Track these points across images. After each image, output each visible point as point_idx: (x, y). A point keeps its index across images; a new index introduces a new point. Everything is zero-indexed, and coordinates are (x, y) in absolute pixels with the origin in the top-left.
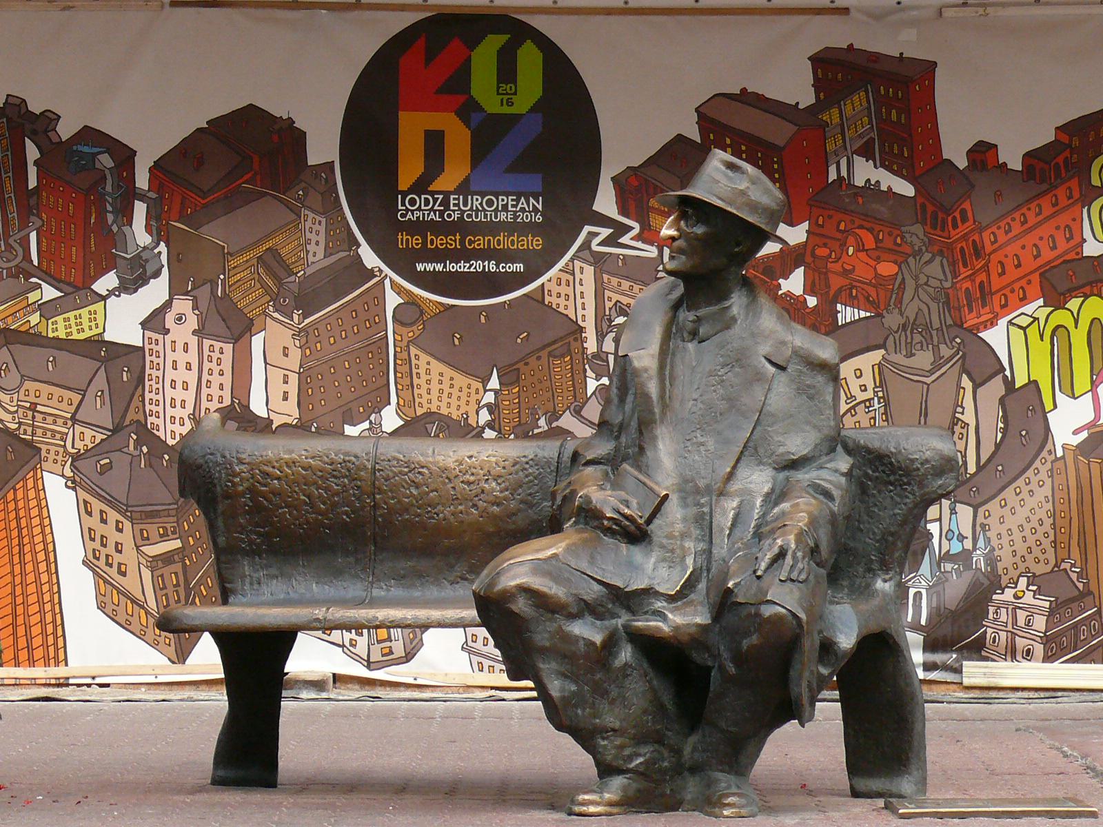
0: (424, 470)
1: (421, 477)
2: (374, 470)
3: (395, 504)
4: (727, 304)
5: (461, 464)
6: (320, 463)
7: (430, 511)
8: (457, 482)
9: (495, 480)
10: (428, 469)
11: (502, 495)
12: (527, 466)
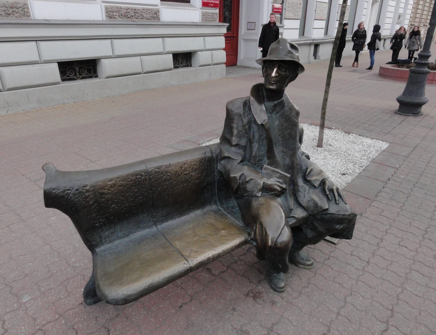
0: (168, 174)
2: (150, 179)
4: (283, 99)
5: (182, 168)
7: (174, 189)
10: (171, 173)
11: (199, 176)
12: (205, 162)
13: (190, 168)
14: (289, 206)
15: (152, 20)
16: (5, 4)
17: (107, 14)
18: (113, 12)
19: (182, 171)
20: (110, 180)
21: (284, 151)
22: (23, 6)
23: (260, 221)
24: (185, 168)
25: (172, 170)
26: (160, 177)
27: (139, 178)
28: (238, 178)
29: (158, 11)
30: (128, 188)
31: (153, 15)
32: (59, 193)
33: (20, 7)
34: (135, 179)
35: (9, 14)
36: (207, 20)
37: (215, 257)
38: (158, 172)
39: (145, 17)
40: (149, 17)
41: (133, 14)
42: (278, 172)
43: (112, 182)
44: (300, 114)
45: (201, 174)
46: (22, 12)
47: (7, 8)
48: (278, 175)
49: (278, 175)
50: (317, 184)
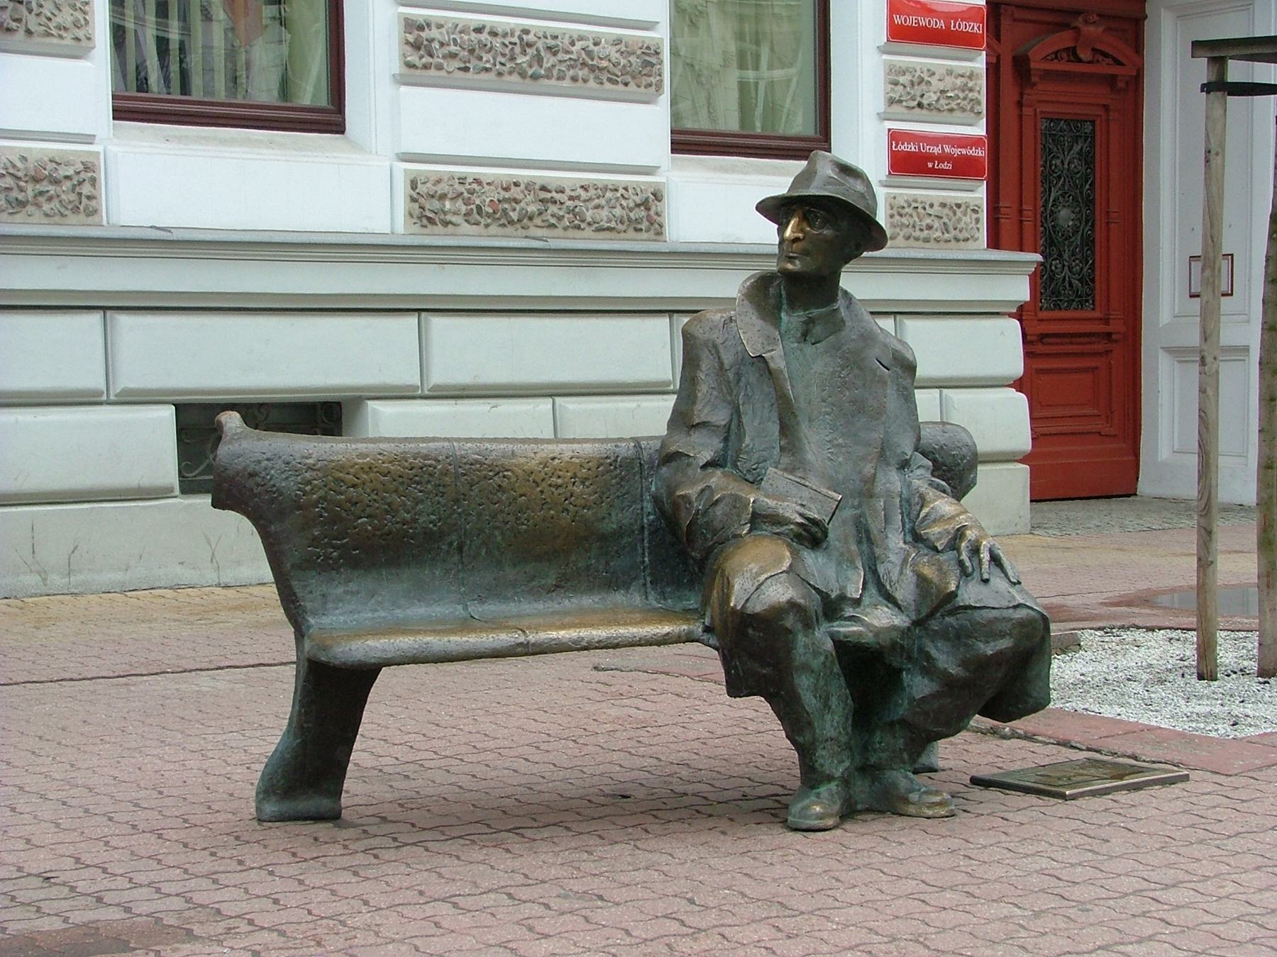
5: (546, 466)
9: (583, 483)
10: (512, 472)
15: (622, 235)
16: (14, 166)
17: (416, 205)
18: (443, 197)
22: (78, 173)
27: (430, 466)
29: (658, 196)
31: (631, 210)
33: (67, 177)
35: (22, 204)
36: (917, 239)
38: (482, 464)
39: (589, 219)
40: (609, 221)
41: (532, 208)
46: (73, 197)
47: (19, 178)
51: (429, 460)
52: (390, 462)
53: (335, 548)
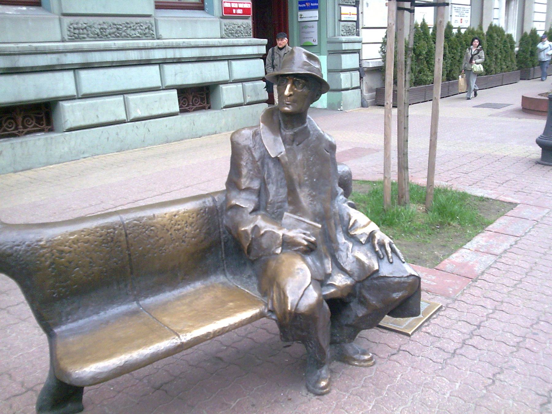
1: (153, 232)
3: (142, 249)
4: (305, 125)
6: (94, 237)
8: (172, 231)
9: (190, 225)
12: (204, 214)
13: (183, 221)
14: (325, 270)
19: (172, 225)
20: (72, 234)
21: (312, 194)
23: (277, 282)
24: (177, 221)
25: (157, 223)
26: (141, 232)
27: (111, 232)
28: (249, 232)
30: (96, 245)
32: (5, 250)
34: (106, 233)
37: (217, 332)
38: (139, 226)
42: (304, 222)
43: (74, 237)
44: (337, 146)
45: (200, 231)
48: (304, 225)
49: (304, 225)
50: (363, 240)
51: (110, 229)
52: (88, 235)
53: (64, 287)
